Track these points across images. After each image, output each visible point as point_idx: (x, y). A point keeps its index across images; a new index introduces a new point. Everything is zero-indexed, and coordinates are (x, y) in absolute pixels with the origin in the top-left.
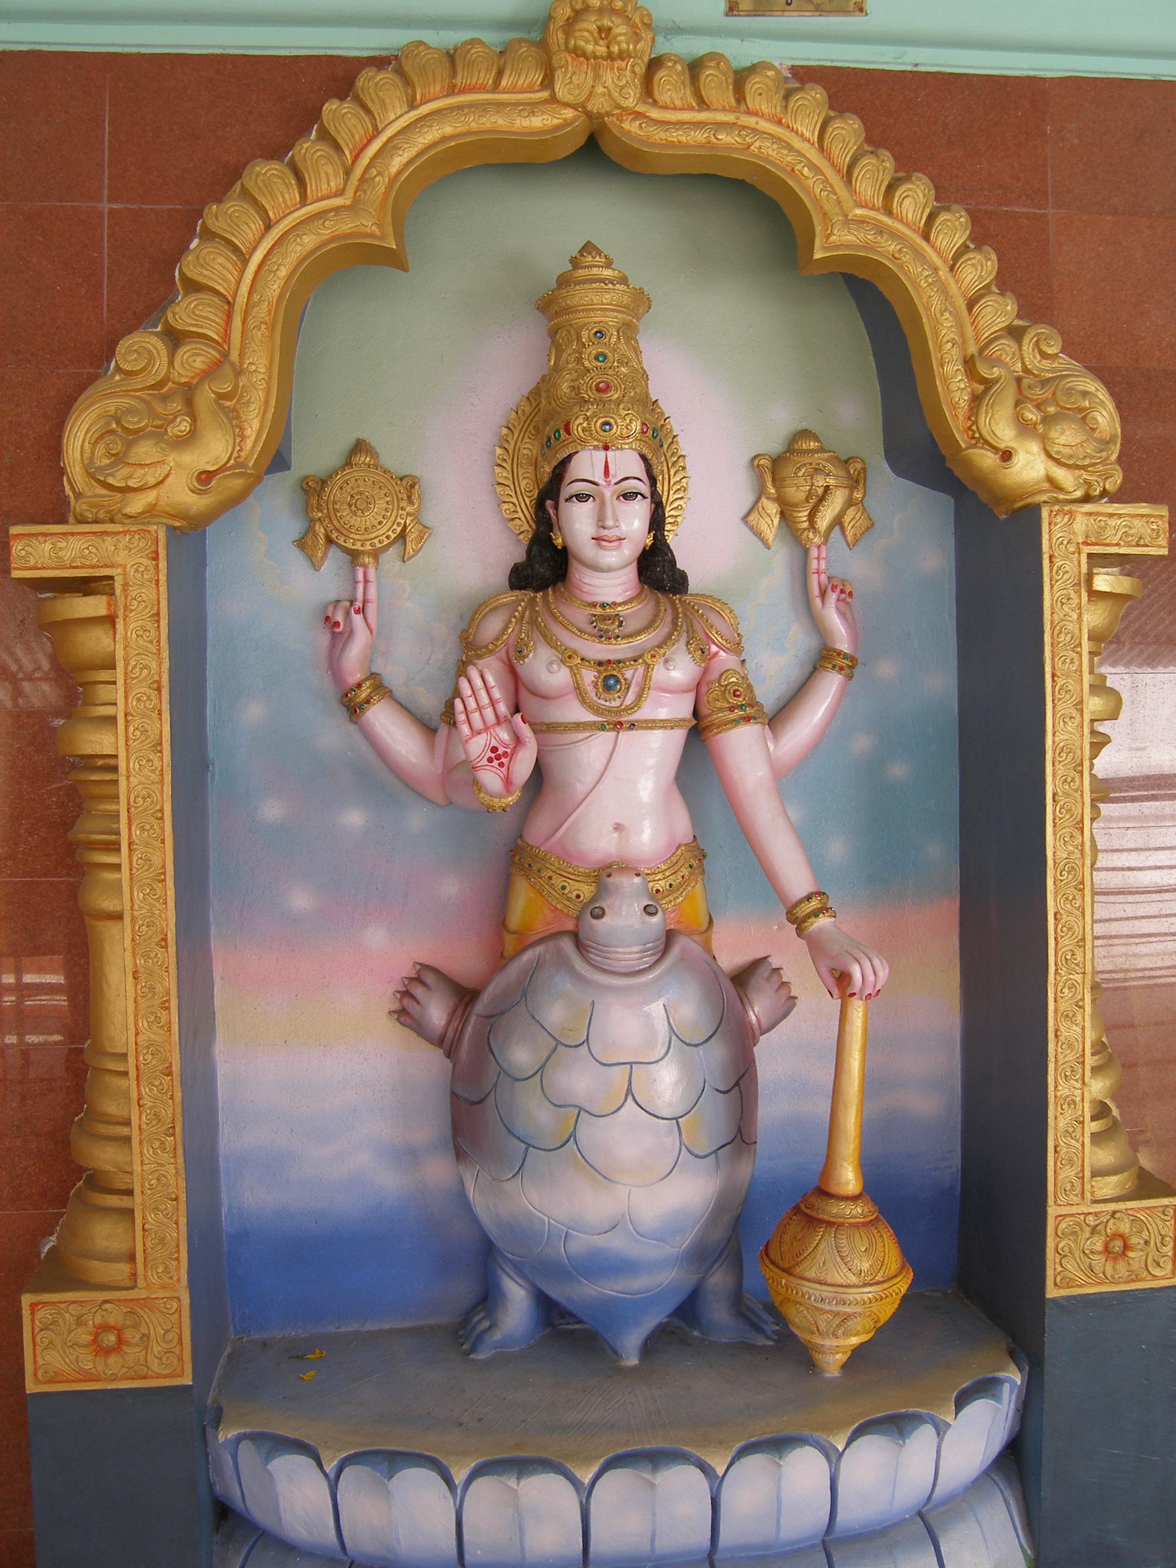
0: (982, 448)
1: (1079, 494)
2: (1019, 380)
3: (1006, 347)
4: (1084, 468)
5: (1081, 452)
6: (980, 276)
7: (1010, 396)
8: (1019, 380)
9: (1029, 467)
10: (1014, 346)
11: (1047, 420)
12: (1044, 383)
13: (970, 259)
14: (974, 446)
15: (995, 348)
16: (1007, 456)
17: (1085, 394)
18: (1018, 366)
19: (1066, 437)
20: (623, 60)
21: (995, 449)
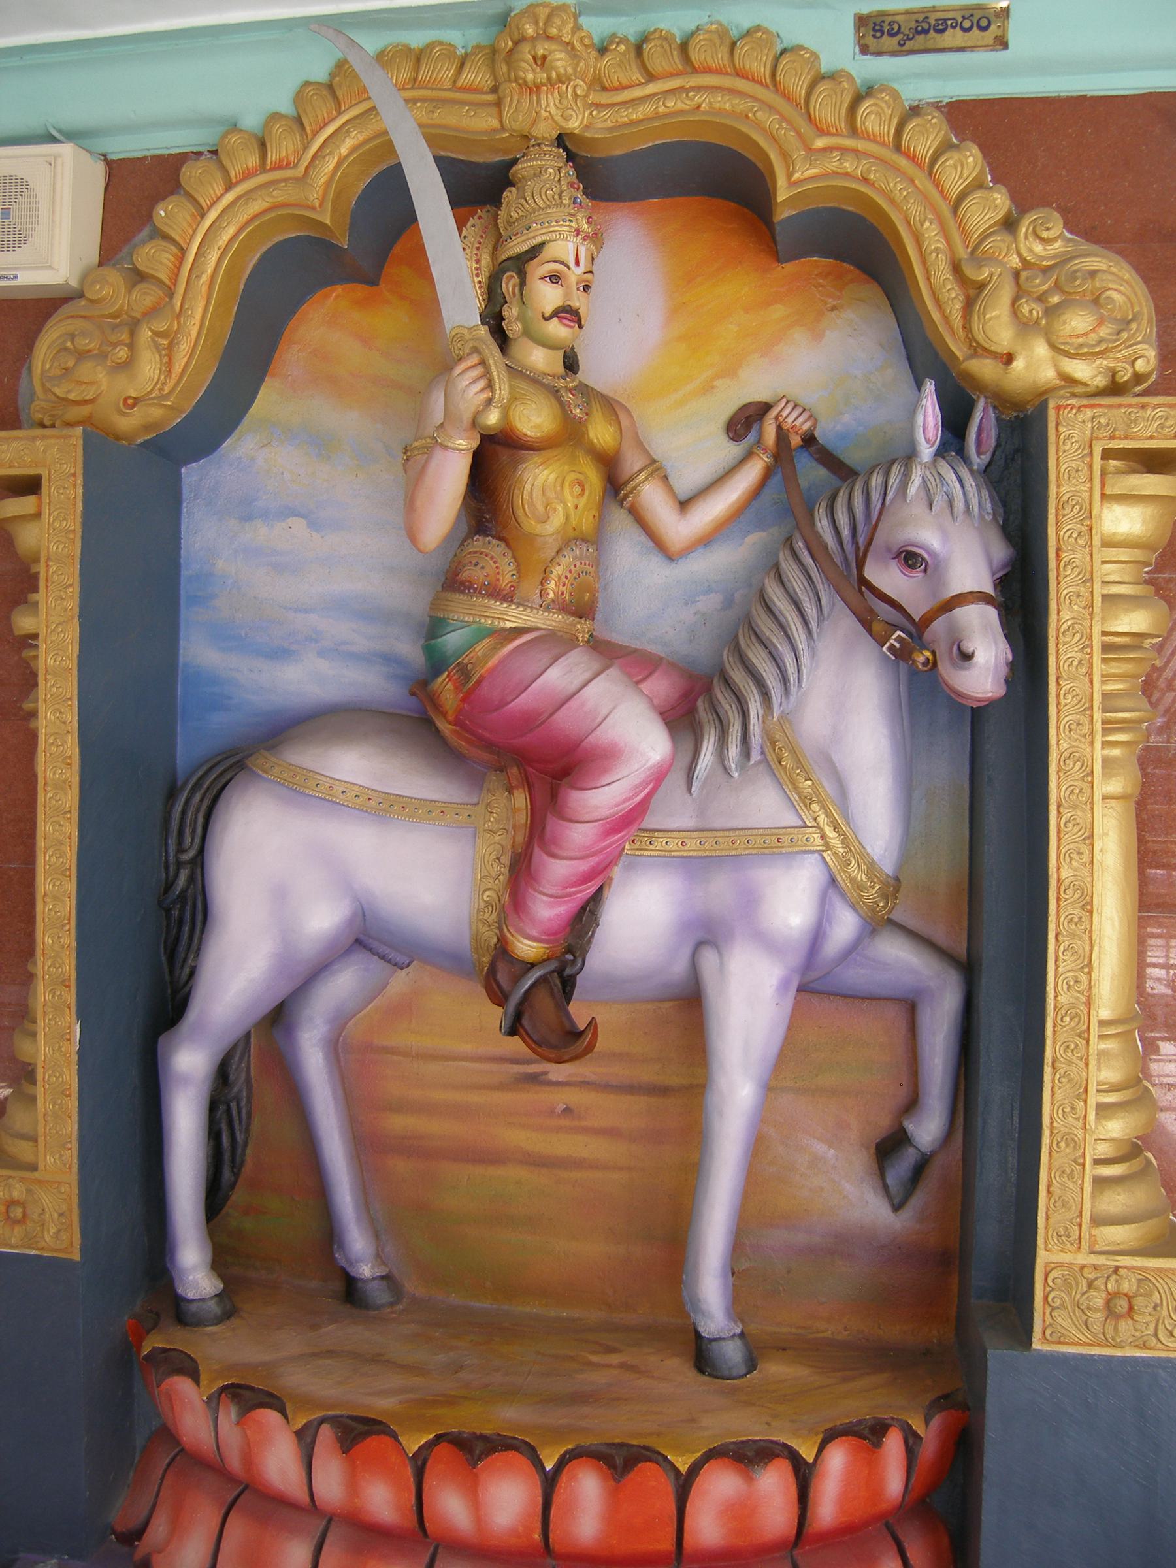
0: (982, 356)
1: (1101, 382)
2: (1017, 274)
3: (999, 242)
4: (1102, 353)
5: (1093, 339)
6: (961, 176)
7: (1006, 294)
8: (1017, 274)
9: (1034, 366)
10: (1008, 238)
11: (1052, 312)
12: (1046, 270)
13: (946, 160)
14: (971, 357)
15: (987, 245)
16: (1009, 359)
17: (1093, 274)
18: (1015, 261)
19: (1077, 322)
20: (563, 83)
21: (995, 355)
